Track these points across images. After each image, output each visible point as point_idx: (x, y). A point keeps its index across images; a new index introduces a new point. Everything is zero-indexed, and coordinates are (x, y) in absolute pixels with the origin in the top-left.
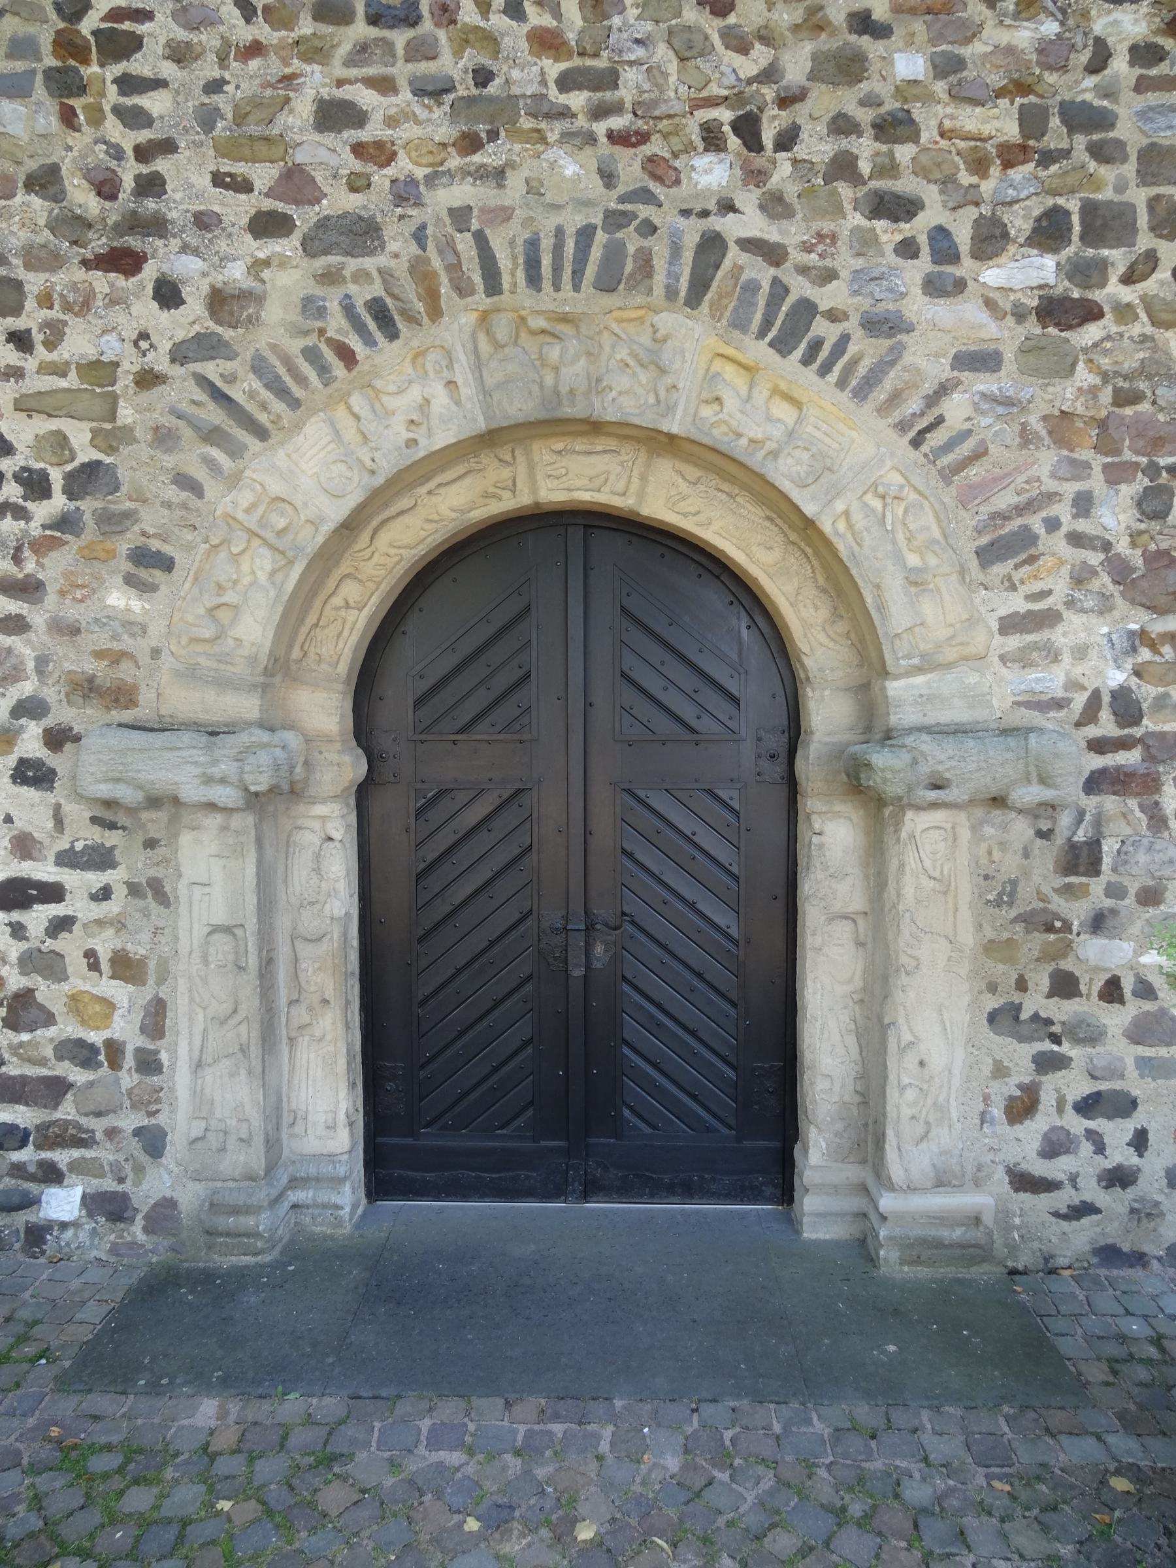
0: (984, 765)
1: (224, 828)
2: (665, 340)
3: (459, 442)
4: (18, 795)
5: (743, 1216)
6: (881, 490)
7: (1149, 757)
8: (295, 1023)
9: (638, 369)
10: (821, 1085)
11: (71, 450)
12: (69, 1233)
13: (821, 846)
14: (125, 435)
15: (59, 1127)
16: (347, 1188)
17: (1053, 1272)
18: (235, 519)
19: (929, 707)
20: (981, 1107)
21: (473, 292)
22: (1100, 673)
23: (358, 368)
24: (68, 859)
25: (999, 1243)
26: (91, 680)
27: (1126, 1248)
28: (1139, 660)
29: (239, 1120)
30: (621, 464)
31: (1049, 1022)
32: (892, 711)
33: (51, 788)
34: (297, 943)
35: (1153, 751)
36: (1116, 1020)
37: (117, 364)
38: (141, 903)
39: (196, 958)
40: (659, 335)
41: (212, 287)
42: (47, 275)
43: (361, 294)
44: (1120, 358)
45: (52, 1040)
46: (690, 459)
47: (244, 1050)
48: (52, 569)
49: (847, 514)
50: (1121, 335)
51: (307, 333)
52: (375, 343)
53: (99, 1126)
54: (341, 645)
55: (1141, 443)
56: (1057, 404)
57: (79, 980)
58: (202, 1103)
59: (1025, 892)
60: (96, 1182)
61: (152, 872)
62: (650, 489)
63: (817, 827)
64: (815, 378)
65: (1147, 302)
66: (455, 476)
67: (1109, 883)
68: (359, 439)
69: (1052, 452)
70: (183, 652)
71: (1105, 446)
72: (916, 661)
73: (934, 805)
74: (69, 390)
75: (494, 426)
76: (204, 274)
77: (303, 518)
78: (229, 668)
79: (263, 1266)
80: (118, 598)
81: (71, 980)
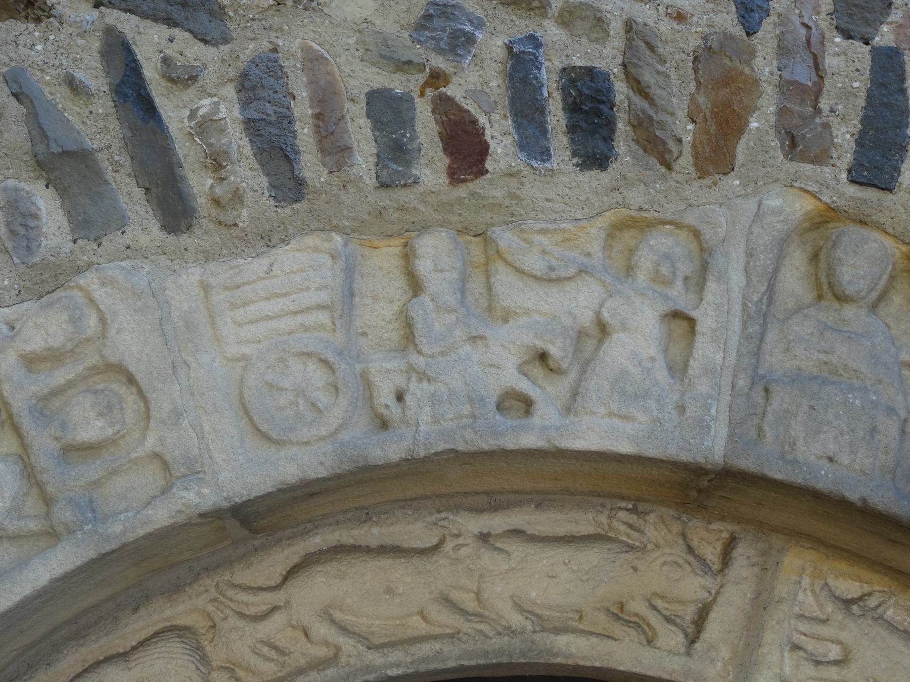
21: (821, 158)
23: (476, 185)
51: (405, 66)
52: (545, 154)
66: (562, 530)
68: (393, 335)
75: (747, 464)
77: (151, 442)
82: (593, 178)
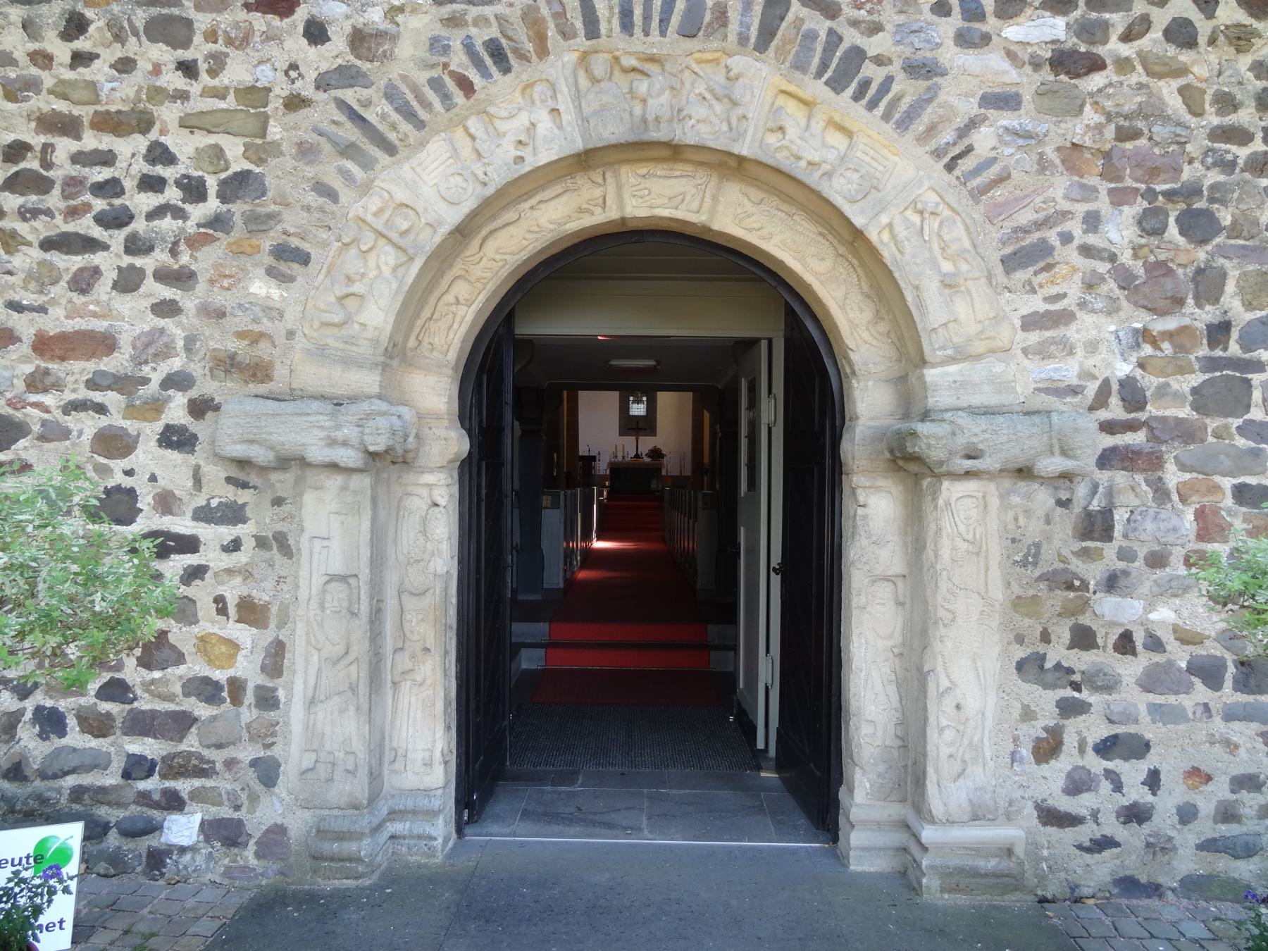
1: (344, 488)
2: (737, 79)
3: (560, 160)
4: (163, 457)
5: (794, 852)
6: (919, 206)
7: (1153, 438)
8: (399, 669)
9: (714, 102)
10: (866, 730)
11: (226, 161)
12: (187, 857)
13: (865, 517)
14: (273, 149)
15: (183, 758)
16: (440, 821)
17: (1078, 900)
18: (364, 221)
19: (962, 391)
20: (1011, 747)
21: (575, 36)
22: (1109, 365)
23: (476, 96)
24: (203, 514)
25: (1029, 874)
26: (233, 357)
27: (1143, 879)
28: (1143, 354)
29: (347, 753)
30: (696, 186)
31: (1070, 671)
32: (930, 393)
33: (192, 452)
34: (403, 597)
35: (1157, 432)
36: (1130, 669)
37: (269, 90)
38: (266, 555)
39: (314, 604)
40: (731, 74)
41: (354, 27)
42: (214, 15)
43: (480, 36)
44: (1122, 101)
45: (181, 677)
46: (755, 182)
47: (353, 689)
48: (204, 261)
49: (890, 226)
50: (1121, 83)
51: (433, 66)
52: (491, 76)
53: (218, 756)
54: (451, 336)
55: (1140, 172)
56: (1069, 138)
57: (209, 624)
58: (313, 735)
59: (1048, 553)
60: (213, 809)
61: (279, 527)
62: (720, 208)
63: (861, 499)
64: (863, 111)
65: (1143, 57)
67: (1120, 548)
68: (474, 156)
69: (1065, 178)
70: (314, 334)
71: (1110, 172)
72: (950, 352)
73: (968, 474)
74: (227, 110)
75: (590, 146)
76: (347, 17)
78: (356, 349)
79: (364, 889)
80: (261, 287)
81: (201, 623)
82: (509, 77)
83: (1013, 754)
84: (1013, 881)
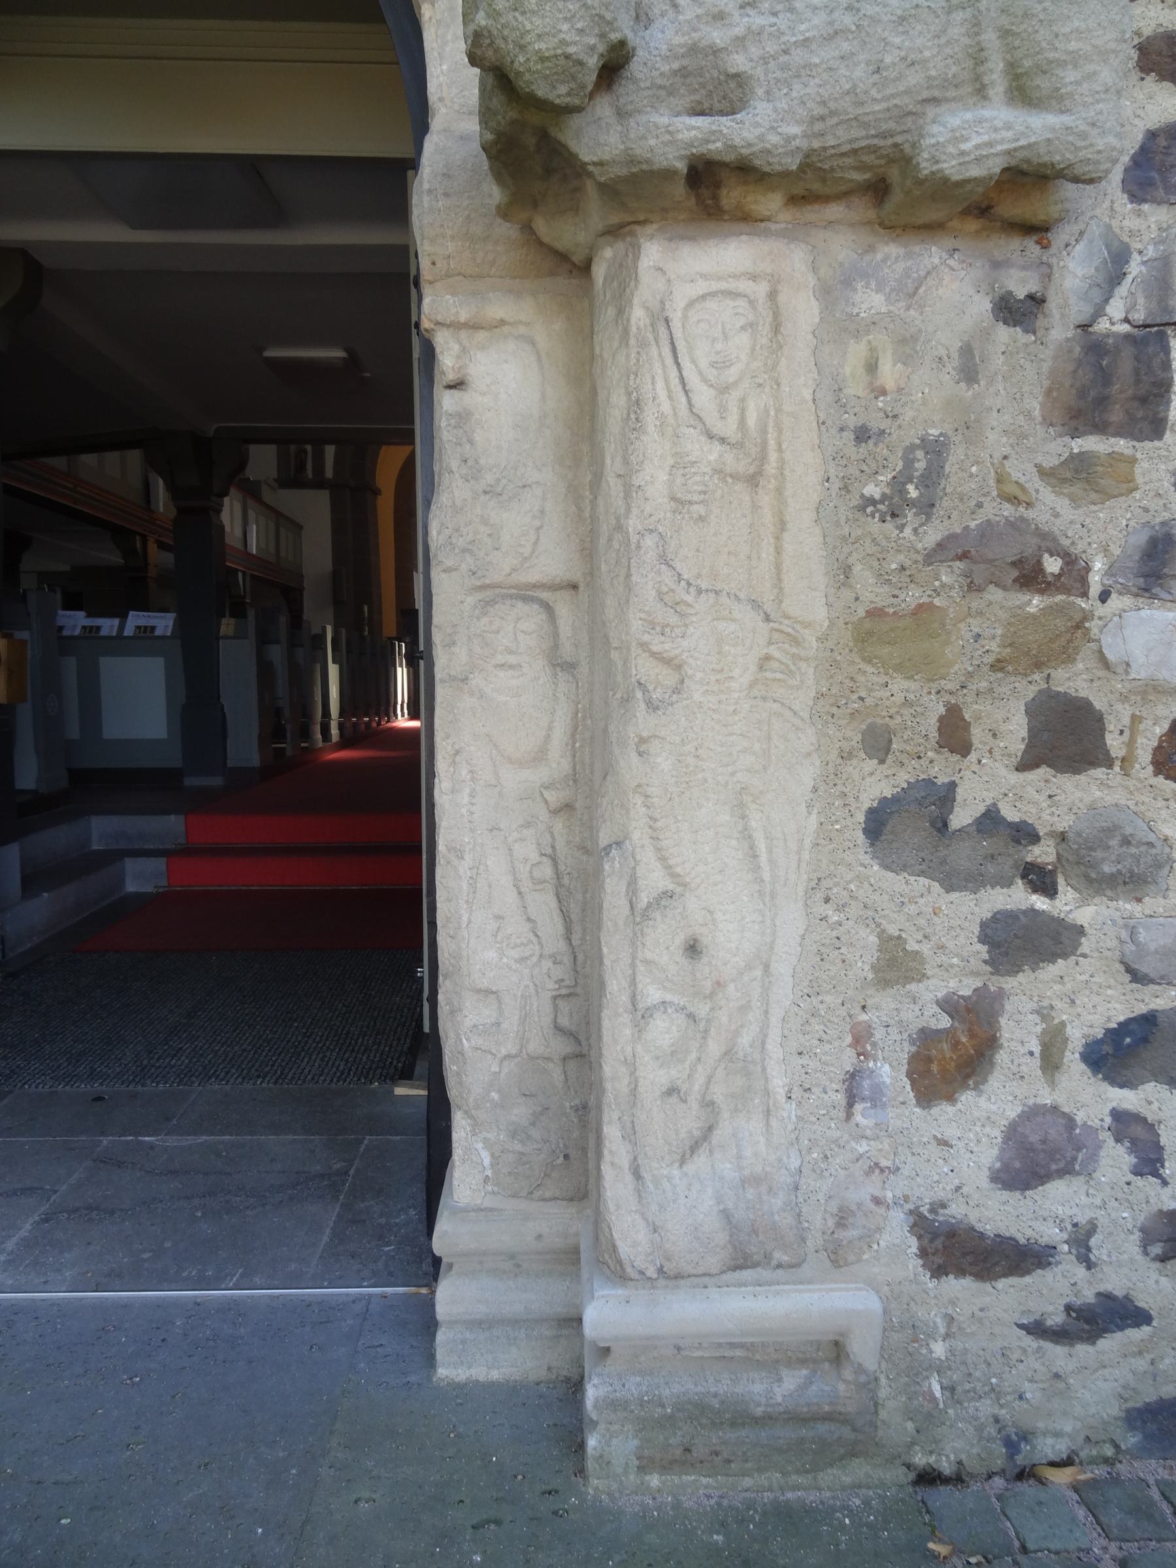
0: (848, 20)
13: (463, 417)
20: (849, 1060)
31: (1025, 834)
59: (965, 474)
83: (853, 1078)
84: (846, 1433)
